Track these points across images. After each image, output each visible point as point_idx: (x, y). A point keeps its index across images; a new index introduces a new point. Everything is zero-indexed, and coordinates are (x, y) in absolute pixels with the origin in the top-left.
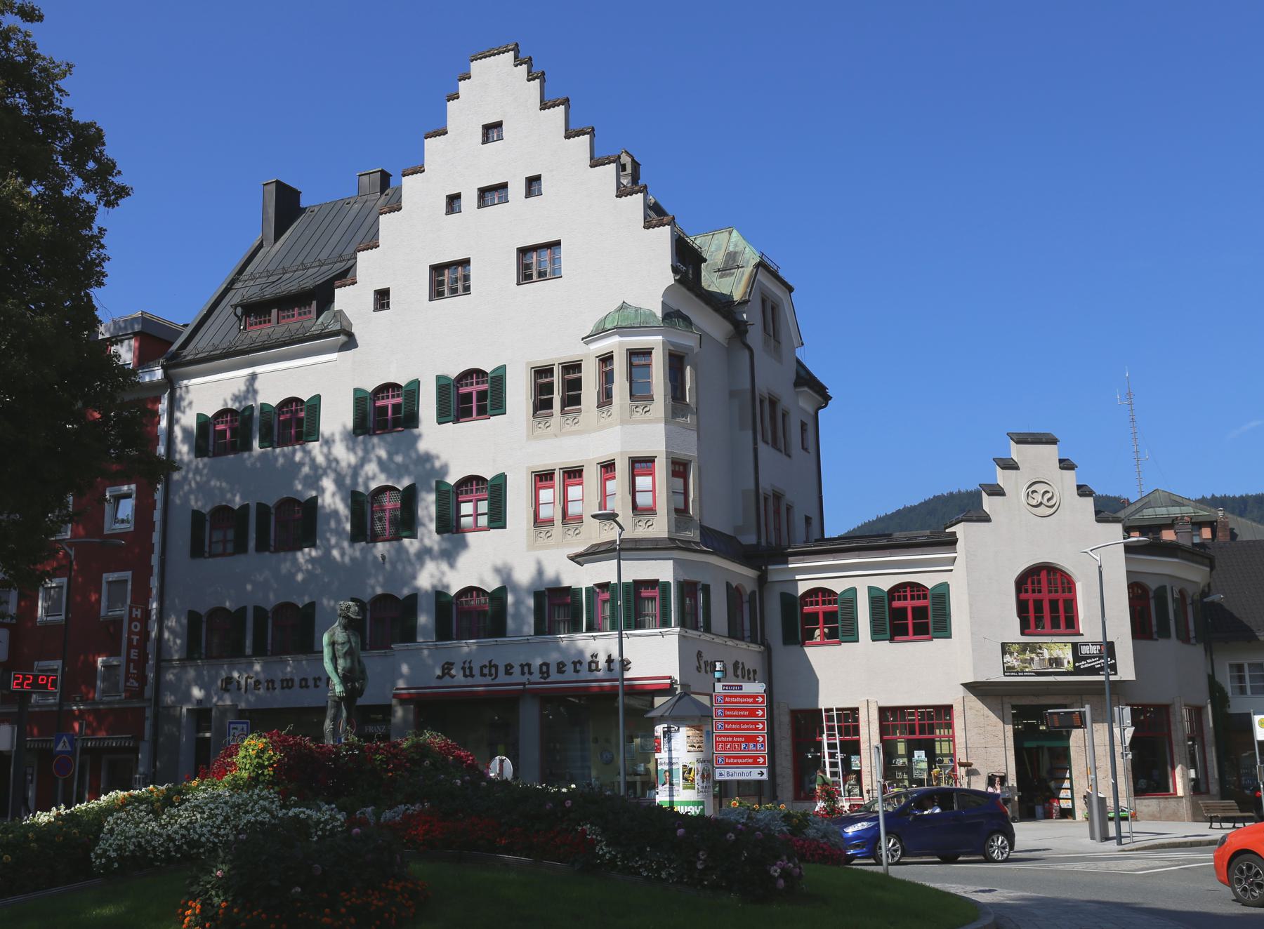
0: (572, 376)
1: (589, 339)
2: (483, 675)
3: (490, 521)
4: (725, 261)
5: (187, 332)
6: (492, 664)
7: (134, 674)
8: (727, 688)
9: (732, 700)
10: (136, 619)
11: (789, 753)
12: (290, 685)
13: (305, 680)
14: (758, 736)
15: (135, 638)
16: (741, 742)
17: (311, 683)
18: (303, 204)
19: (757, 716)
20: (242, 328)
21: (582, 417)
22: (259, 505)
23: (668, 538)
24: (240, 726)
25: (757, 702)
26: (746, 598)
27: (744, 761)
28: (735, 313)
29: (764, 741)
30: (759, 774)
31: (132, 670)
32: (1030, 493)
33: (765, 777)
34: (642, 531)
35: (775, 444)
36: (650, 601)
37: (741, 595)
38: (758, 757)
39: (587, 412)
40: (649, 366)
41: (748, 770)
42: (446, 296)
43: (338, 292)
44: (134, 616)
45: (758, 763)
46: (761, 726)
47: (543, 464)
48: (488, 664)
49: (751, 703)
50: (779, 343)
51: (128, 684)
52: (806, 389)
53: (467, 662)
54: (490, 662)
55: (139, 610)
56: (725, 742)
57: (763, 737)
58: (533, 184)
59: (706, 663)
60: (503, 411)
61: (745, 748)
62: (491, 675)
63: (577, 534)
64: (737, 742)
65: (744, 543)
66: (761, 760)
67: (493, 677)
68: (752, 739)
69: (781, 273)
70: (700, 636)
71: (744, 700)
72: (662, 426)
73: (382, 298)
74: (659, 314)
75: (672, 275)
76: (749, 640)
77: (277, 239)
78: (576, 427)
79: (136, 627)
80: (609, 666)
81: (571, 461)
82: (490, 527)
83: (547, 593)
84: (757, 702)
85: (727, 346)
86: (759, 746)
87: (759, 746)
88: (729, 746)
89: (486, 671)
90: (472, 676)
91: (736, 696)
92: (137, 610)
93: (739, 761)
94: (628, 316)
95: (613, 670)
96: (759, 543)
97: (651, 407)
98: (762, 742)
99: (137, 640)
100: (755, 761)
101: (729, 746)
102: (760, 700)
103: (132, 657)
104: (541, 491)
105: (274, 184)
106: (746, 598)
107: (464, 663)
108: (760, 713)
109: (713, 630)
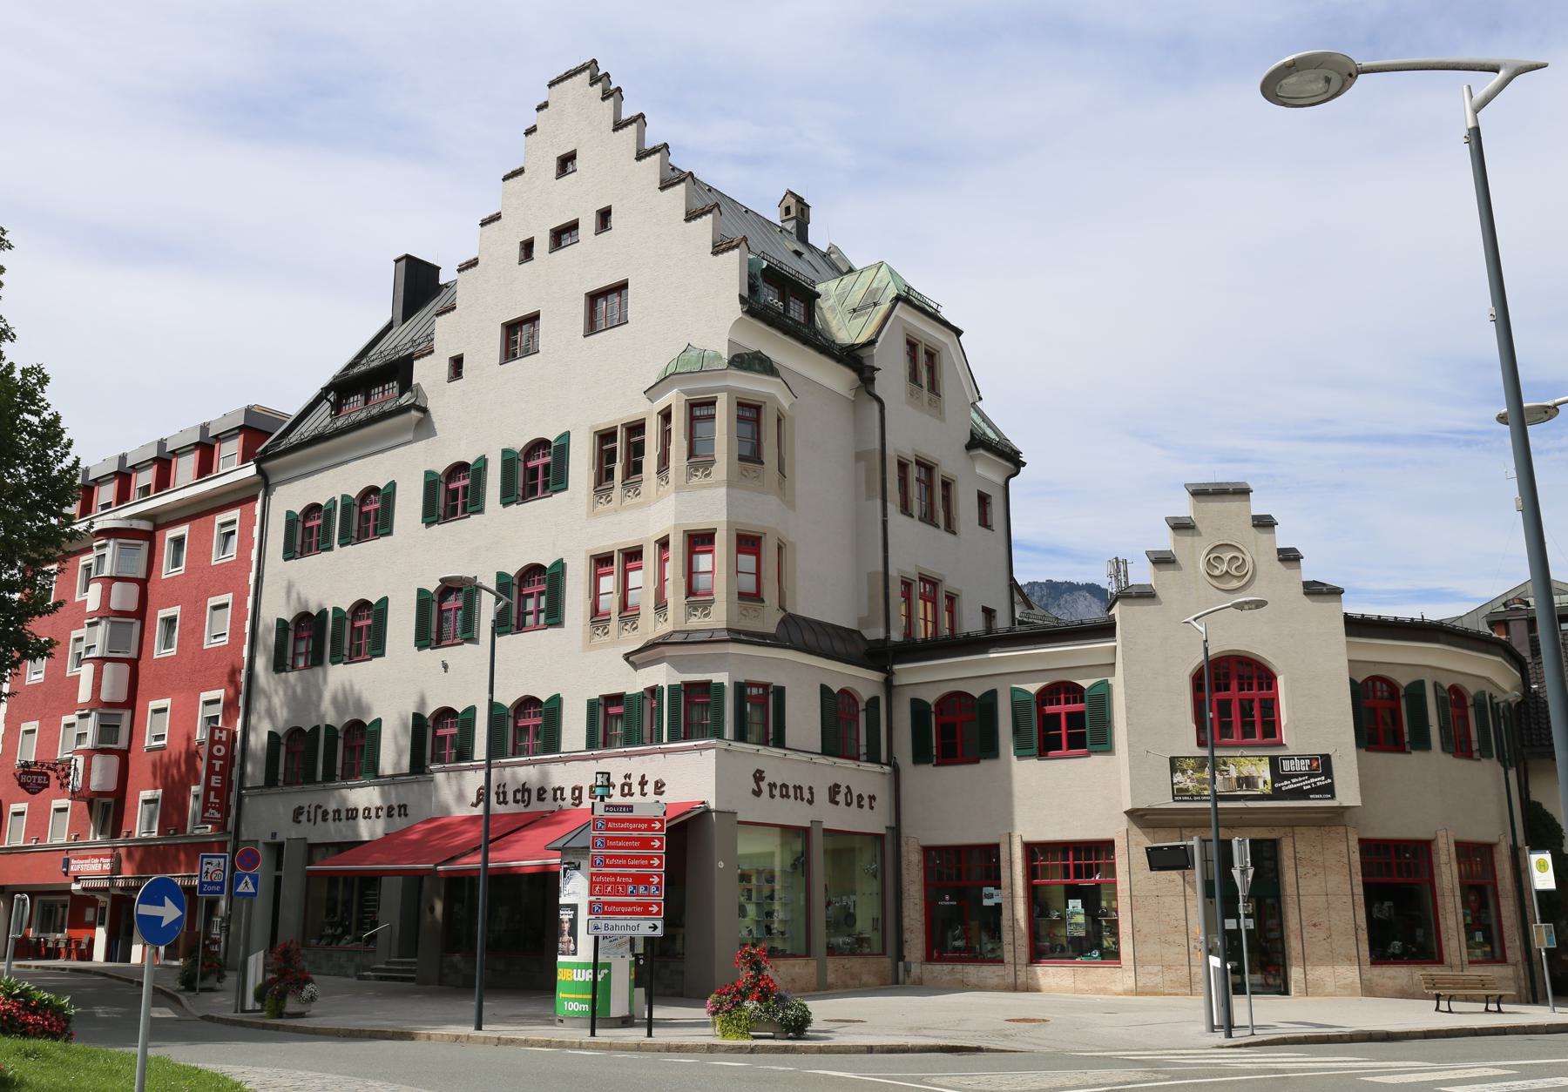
0: (637, 439)
1: (651, 392)
2: (516, 801)
3: (547, 618)
5: (289, 422)
7: (215, 803)
10: (220, 741)
13: (369, 810)
14: (651, 876)
15: (218, 763)
16: (627, 883)
18: (442, 282)
19: (652, 848)
21: (643, 488)
22: (335, 609)
23: (727, 629)
24: (215, 861)
25: (653, 829)
26: (862, 706)
27: (630, 910)
28: (862, 358)
29: (660, 883)
30: (650, 927)
31: (212, 799)
32: (1211, 560)
33: (659, 932)
34: (697, 622)
35: (928, 518)
37: (856, 703)
38: (650, 905)
40: (713, 417)
41: (635, 923)
43: (416, 364)
44: (216, 738)
45: (650, 913)
46: (656, 862)
47: (602, 546)
52: (981, 451)
55: (225, 732)
56: (604, 883)
57: (660, 876)
58: (604, 217)
59: (772, 786)
60: (564, 485)
61: (632, 892)
62: (523, 802)
64: (622, 883)
65: (868, 639)
66: (655, 909)
68: (643, 880)
69: (945, 314)
70: (758, 750)
71: (635, 826)
72: (723, 490)
73: (457, 364)
74: (725, 356)
75: (739, 306)
76: (864, 758)
79: (219, 750)
80: (642, 789)
81: (630, 541)
82: (549, 625)
84: (653, 829)
85: (853, 399)
86: (653, 889)
87: (653, 889)
88: (609, 889)
90: (505, 803)
94: (689, 360)
96: (887, 638)
97: (712, 469)
100: (645, 910)
101: (609, 889)
103: (213, 784)
104: (602, 579)
106: (862, 706)
108: (657, 844)
109: (790, 740)
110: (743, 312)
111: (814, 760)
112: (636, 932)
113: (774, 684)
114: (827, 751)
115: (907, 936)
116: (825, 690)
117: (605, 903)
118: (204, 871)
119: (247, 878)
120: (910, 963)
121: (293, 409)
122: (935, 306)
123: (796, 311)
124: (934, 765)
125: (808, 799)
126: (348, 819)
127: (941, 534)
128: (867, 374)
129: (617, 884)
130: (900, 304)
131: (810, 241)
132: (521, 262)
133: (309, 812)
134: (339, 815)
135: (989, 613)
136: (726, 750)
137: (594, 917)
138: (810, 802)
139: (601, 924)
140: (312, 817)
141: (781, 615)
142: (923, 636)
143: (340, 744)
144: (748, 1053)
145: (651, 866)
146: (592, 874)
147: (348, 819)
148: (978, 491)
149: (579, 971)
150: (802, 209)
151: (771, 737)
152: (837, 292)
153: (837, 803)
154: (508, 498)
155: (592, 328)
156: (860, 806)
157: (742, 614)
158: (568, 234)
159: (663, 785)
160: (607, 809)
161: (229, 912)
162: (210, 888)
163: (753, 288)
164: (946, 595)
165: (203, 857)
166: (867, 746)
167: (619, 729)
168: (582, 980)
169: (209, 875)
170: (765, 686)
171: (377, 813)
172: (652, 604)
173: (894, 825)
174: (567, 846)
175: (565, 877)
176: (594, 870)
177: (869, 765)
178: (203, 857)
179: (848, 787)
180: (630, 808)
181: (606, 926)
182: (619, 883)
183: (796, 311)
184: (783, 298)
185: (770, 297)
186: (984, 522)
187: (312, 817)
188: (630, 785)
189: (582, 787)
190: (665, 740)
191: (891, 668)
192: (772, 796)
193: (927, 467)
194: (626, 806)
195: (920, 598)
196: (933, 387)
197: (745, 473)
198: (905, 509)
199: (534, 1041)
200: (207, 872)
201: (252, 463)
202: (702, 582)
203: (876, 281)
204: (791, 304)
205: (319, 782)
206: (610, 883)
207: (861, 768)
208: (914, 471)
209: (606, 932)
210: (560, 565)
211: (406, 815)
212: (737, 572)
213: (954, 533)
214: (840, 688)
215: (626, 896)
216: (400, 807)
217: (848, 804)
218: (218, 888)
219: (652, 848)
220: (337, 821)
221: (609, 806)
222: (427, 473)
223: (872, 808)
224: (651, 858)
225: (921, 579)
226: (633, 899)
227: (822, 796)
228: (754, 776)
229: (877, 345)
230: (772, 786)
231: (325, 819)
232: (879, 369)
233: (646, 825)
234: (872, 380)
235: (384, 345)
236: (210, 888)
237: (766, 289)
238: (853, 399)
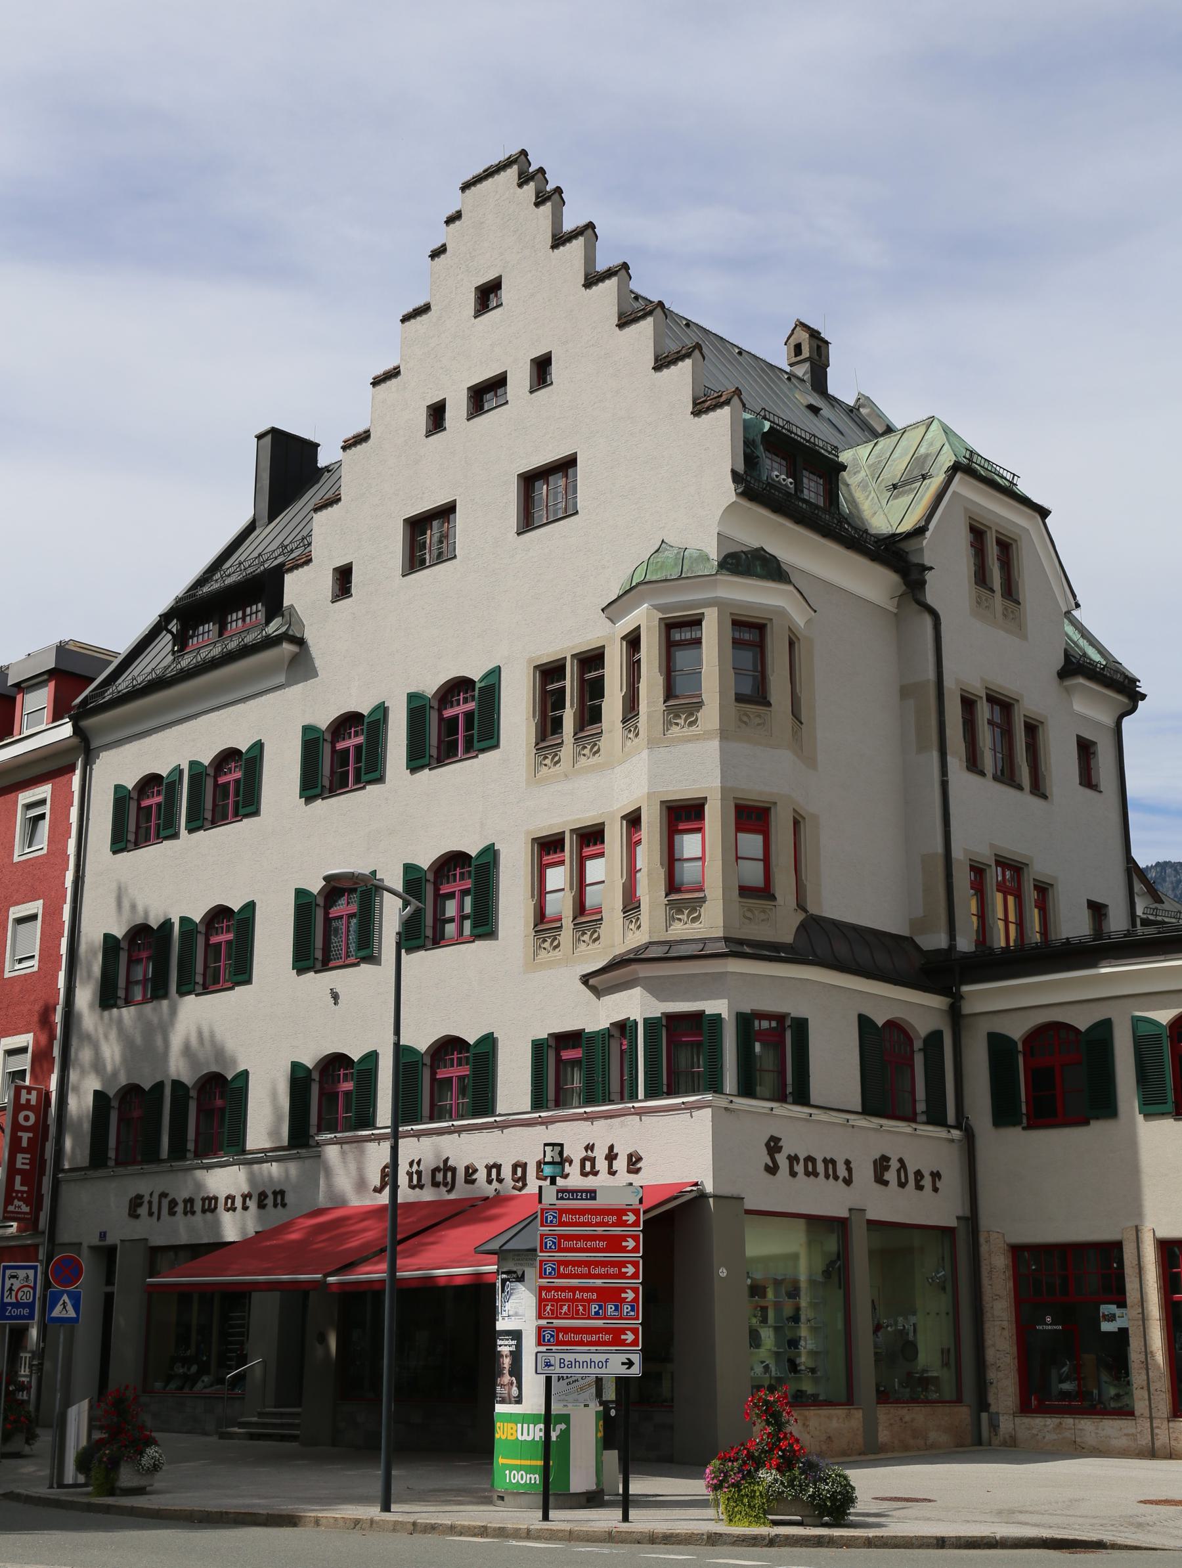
0: (593, 674)
1: (612, 609)
2: (435, 1184)
3: (474, 926)
4: (909, 471)
7: (22, 1192)
8: (566, 1195)
9: (575, 1218)
11: (1005, 1324)
13: (233, 1198)
14: (623, 1290)
15: (25, 1136)
16: (590, 1301)
18: (322, 462)
19: (624, 1250)
20: (176, 648)
21: (603, 743)
22: (184, 920)
23: (724, 937)
25: (624, 1223)
26: (918, 1044)
27: (594, 1338)
28: (907, 553)
29: (636, 1299)
30: (623, 1364)
31: (18, 1186)
33: (636, 1370)
34: (682, 929)
35: (1007, 776)
36: (695, 1050)
37: (910, 1041)
38: (623, 1331)
40: (698, 642)
41: (603, 1357)
42: (428, 564)
43: (288, 578)
44: (23, 1101)
45: (623, 1343)
46: (630, 1270)
47: (548, 825)
49: (614, 1225)
50: (1019, 603)
51: (11, 1208)
52: (1081, 680)
53: (415, 1164)
55: (34, 1093)
56: (558, 1301)
57: (635, 1290)
58: (542, 368)
59: (793, 1159)
61: (597, 1313)
62: (446, 1185)
64: (583, 1300)
65: (925, 949)
66: (630, 1337)
67: (449, 1187)
68: (612, 1295)
69: (1024, 487)
70: (772, 1109)
71: (599, 1219)
72: (714, 745)
73: (343, 578)
74: (714, 555)
75: (732, 486)
76: (923, 1118)
78: (594, 760)
79: (27, 1118)
80: (610, 1166)
81: (586, 817)
82: (476, 937)
85: (895, 611)
86: (626, 1308)
87: (626, 1308)
88: (565, 1308)
89: (439, 1177)
90: (421, 1187)
93: (586, 1338)
94: (664, 562)
97: (699, 714)
98: (632, 1301)
99: (29, 1138)
100: (615, 1338)
101: (565, 1308)
103: (19, 1165)
104: (548, 871)
105: (269, 437)
106: (918, 1044)
108: (631, 1244)
109: (815, 1098)
110: (737, 494)
111: (851, 1123)
112: (604, 1370)
113: (792, 1015)
114: (870, 1108)
115: (991, 1375)
116: (864, 1022)
118: (7, 1287)
119: (65, 1297)
120: (997, 1413)
121: (121, 643)
122: (1009, 477)
123: (812, 490)
124: (1024, 1129)
125: (845, 1178)
126: (204, 1211)
128: (914, 576)
129: (574, 1302)
130: (958, 476)
132: (429, 434)
133: (150, 1203)
134: (192, 1206)
135: (1097, 910)
136: (726, 1109)
137: (544, 1349)
138: (848, 1182)
139: (555, 1359)
140: (155, 1209)
141: (800, 917)
142: (1003, 944)
143: (193, 1107)
144: (766, 1546)
145: (623, 1276)
146: (541, 1288)
147: (204, 1211)
148: (1078, 736)
149: (525, 1426)
150: (819, 347)
151: (789, 1089)
152: (871, 461)
153: (886, 1183)
154: (418, 759)
155: (527, 522)
156: (920, 1187)
157: (745, 917)
158: (492, 393)
159: (640, 1159)
161: (42, 1345)
162: (15, 1312)
163: (750, 460)
164: (1035, 885)
165: (5, 1268)
166: (927, 1101)
167: (576, 1081)
168: (530, 1438)
169: (14, 1293)
170: (780, 1018)
171: (244, 1202)
172: (619, 904)
173: (968, 1214)
174: (504, 1248)
175: (503, 1291)
176: (544, 1282)
177: (930, 1128)
178: (5, 1268)
179: (901, 1161)
180: (592, 1194)
182: (578, 1300)
183: (812, 490)
184: (792, 473)
185: (776, 472)
186: (1088, 780)
187: (155, 1209)
188: (593, 1160)
189: (526, 1163)
190: (641, 1095)
191: (958, 990)
192: (793, 1174)
193: (1003, 705)
194: (587, 1191)
195: (998, 890)
196: (1010, 591)
197: (745, 719)
198: (973, 764)
199: (463, 1527)
200: (11, 1289)
201: (68, 720)
202: (688, 873)
203: (924, 443)
204: (805, 480)
205: (163, 1161)
207: (918, 1132)
208: (984, 711)
209: (562, 1371)
210: (490, 854)
211: (284, 1205)
212: (737, 858)
213: (1044, 797)
214: (889, 1017)
215: (589, 1318)
216: (275, 1193)
217: (902, 1185)
218: (26, 1312)
219: (624, 1250)
220: (189, 1215)
222: (307, 729)
223: (936, 1190)
224: (623, 1264)
225: (999, 863)
226: (599, 1323)
227: (864, 1173)
228: (767, 1145)
229: (928, 534)
230: (793, 1159)
231: (172, 1213)
232: (931, 568)
233: (615, 1218)
234: (922, 584)
235: (242, 554)
236: (15, 1312)
237: (768, 462)
238: (895, 611)
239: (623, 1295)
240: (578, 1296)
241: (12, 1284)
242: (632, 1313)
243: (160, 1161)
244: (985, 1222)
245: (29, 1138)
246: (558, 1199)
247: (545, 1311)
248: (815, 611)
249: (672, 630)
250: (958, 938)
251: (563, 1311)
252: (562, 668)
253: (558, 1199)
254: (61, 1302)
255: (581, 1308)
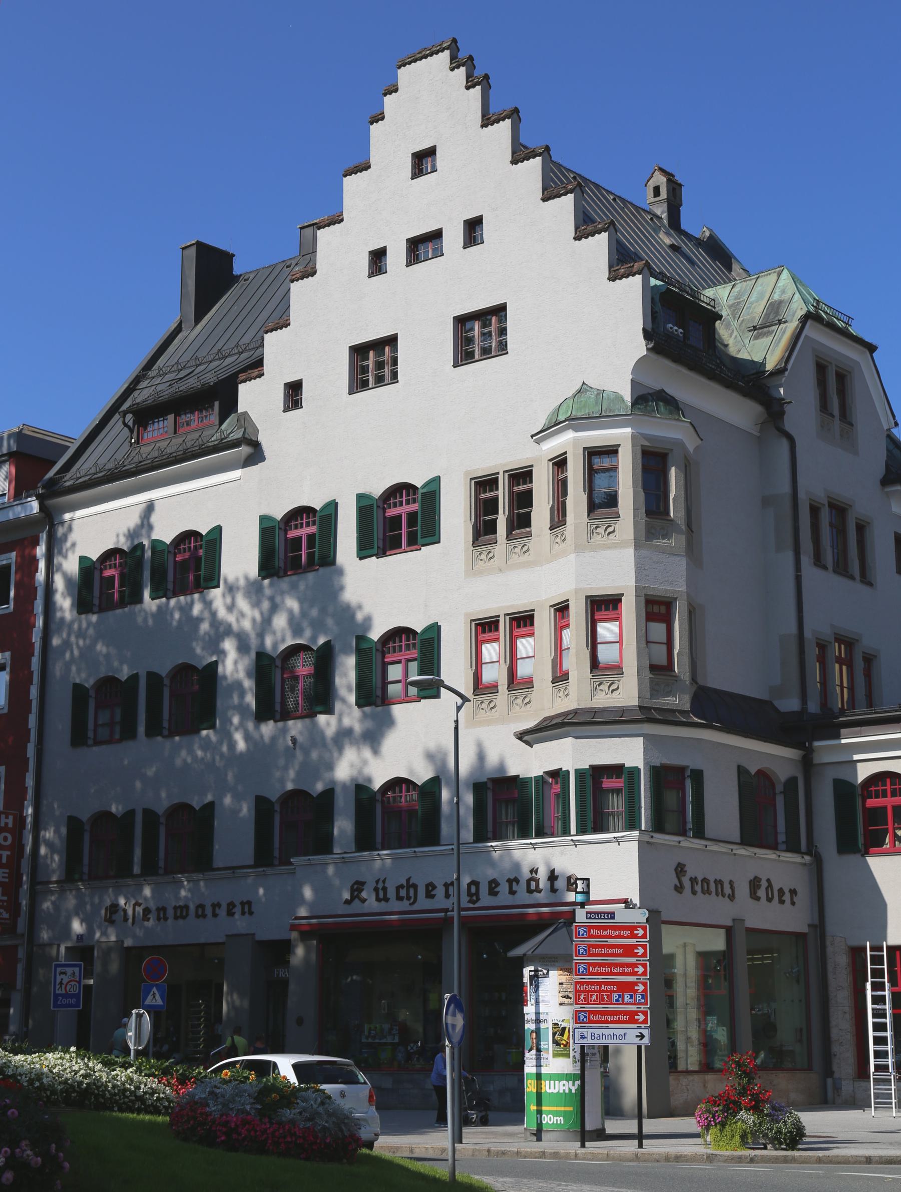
0: (522, 488)
1: (540, 436)
2: (399, 898)
4: (766, 314)
6: (411, 883)
8: (593, 916)
9: (600, 932)
11: (847, 1009)
12: (184, 914)
14: (636, 984)
16: (612, 992)
17: (209, 911)
18: (237, 271)
20: (133, 441)
21: (532, 543)
24: (69, 970)
26: (779, 788)
27: (616, 1018)
28: (769, 387)
29: (645, 991)
30: (637, 1036)
34: (604, 699)
35: (842, 569)
36: (615, 795)
37: (773, 785)
39: (539, 536)
40: (615, 469)
41: (622, 1032)
42: (371, 386)
43: (242, 388)
45: (636, 1022)
46: (641, 970)
47: (485, 608)
48: (405, 885)
49: (628, 937)
50: (852, 425)
53: (381, 882)
54: (408, 880)
55: (11, 817)
56: (589, 991)
57: (645, 984)
59: (693, 880)
60: (435, 539)
61: (617, 1000)
62: (409, 898)
63: (526, 704)
64: (606, 991)
65: (782, 711)
66: (641, 1017)
67: (412, 901)
70: (679, 842)
71: (617, 933)
72: (631, 551)
74: (628, 398)
75: (643, 342)
76: (784, 847)
77: (198, 320)
80: (552, 885)
81: (519, 604)
83: (490, 785)
84: (635, 936)
85: (758, 434)
86: (638, 997)
87: (638, 997)
88: (594, 997)
89: (403, 893)
90: (386, 899)
91: (605, 928)
92: (7, 818)
93: (609, 1018)
94: (586, 401)
95: (557, 890)
96: (804, 710)
97: (617, 526)
98: (642, 992)
99: (7, 855)
100: (631, 1018)
101: (594, 997)
102: (640, 932)
105: (194, 248)
106: (779, 788)
107: (377, 882)
108: (640, 951)
110: (648, 349)
111: (734, 852)
114: (745, 841)
115: (835, 1048)
116: (741, 771)
117: (590, 1012)
118: (58, 981)
119: (155, 989)
120: (840, 1079)
121: (77, 432)
125: (729, 895)
127: (858, 586)
129: (601, 992)
130: (809, 323)
131: (683, 227)
132: (371, 275)
134: (165, 914)
136: (648, 843)
137: (578, 1025)
138: (732, 897)
139: (588, 1033)
142: (840, 706)
144: (748, 1163)
146: (576, 983)
147: (176, 918)
148: (895, 532)
149: (552, 1082)
150: (674, 189)
151: (690, 825)
152: (731, 302)
153: (758, 899)
156: (782, 902)
160: (589, 915)
161: (25, 1029)
162: (66, 1001)
164: (863, 657)
166: (787, 833)
168: (556, 1091)
169: (63, 986)
172: (549, 677)
173: (816, 922)
174: (535, 952)
177: (789, 855)
179: (768, 880)
181: (593, 1035)
182: (604, 991)
188: (537, 881)
190: (573, 830)
191: (811, 744)
192: (694, 892)
193: (839, 510)
194: (608, 913)
195: (837, 662)
199: (527, 1152)
200: (61, 983)
201: (35, 498)
202: (606, 654)
203: (777, 291)
206: (594, 991)
207: (781, 858)
208: (825, 516)
210: (434, 630)
211: (251, 913)
212: (648, 642)
213: (870, 584)
214: (759, 767)
215: (612, 1004)
216: (243, 904)
217: (770, 900)
218: (73, 1001)
219: (636, 955)
221: (591, 913)
222: (263, 519)
223: (793, 903)
224: (634, 965)
226: (599, 1007)
227: (743, 890)
228: (676, 870)
229: (787, 373)
230: (693, 880)
234: (782, 413)
236: (66, 1001)
238: (758, 434)
239: (636, 988)
240: (603, 988)
241: (62, 979)
242: (643, 1001)
243: (131, 875)
244: (830, 928)
245: (7, 855)
246: (587, 918)
247: (579, 999)
248: (702, 440)
249: (593, 457)
250: (809, 703)
251: (593, 999)
252: (496, 481)
253: (587, 918)
254: (152, 993)
255: (605, 997)
